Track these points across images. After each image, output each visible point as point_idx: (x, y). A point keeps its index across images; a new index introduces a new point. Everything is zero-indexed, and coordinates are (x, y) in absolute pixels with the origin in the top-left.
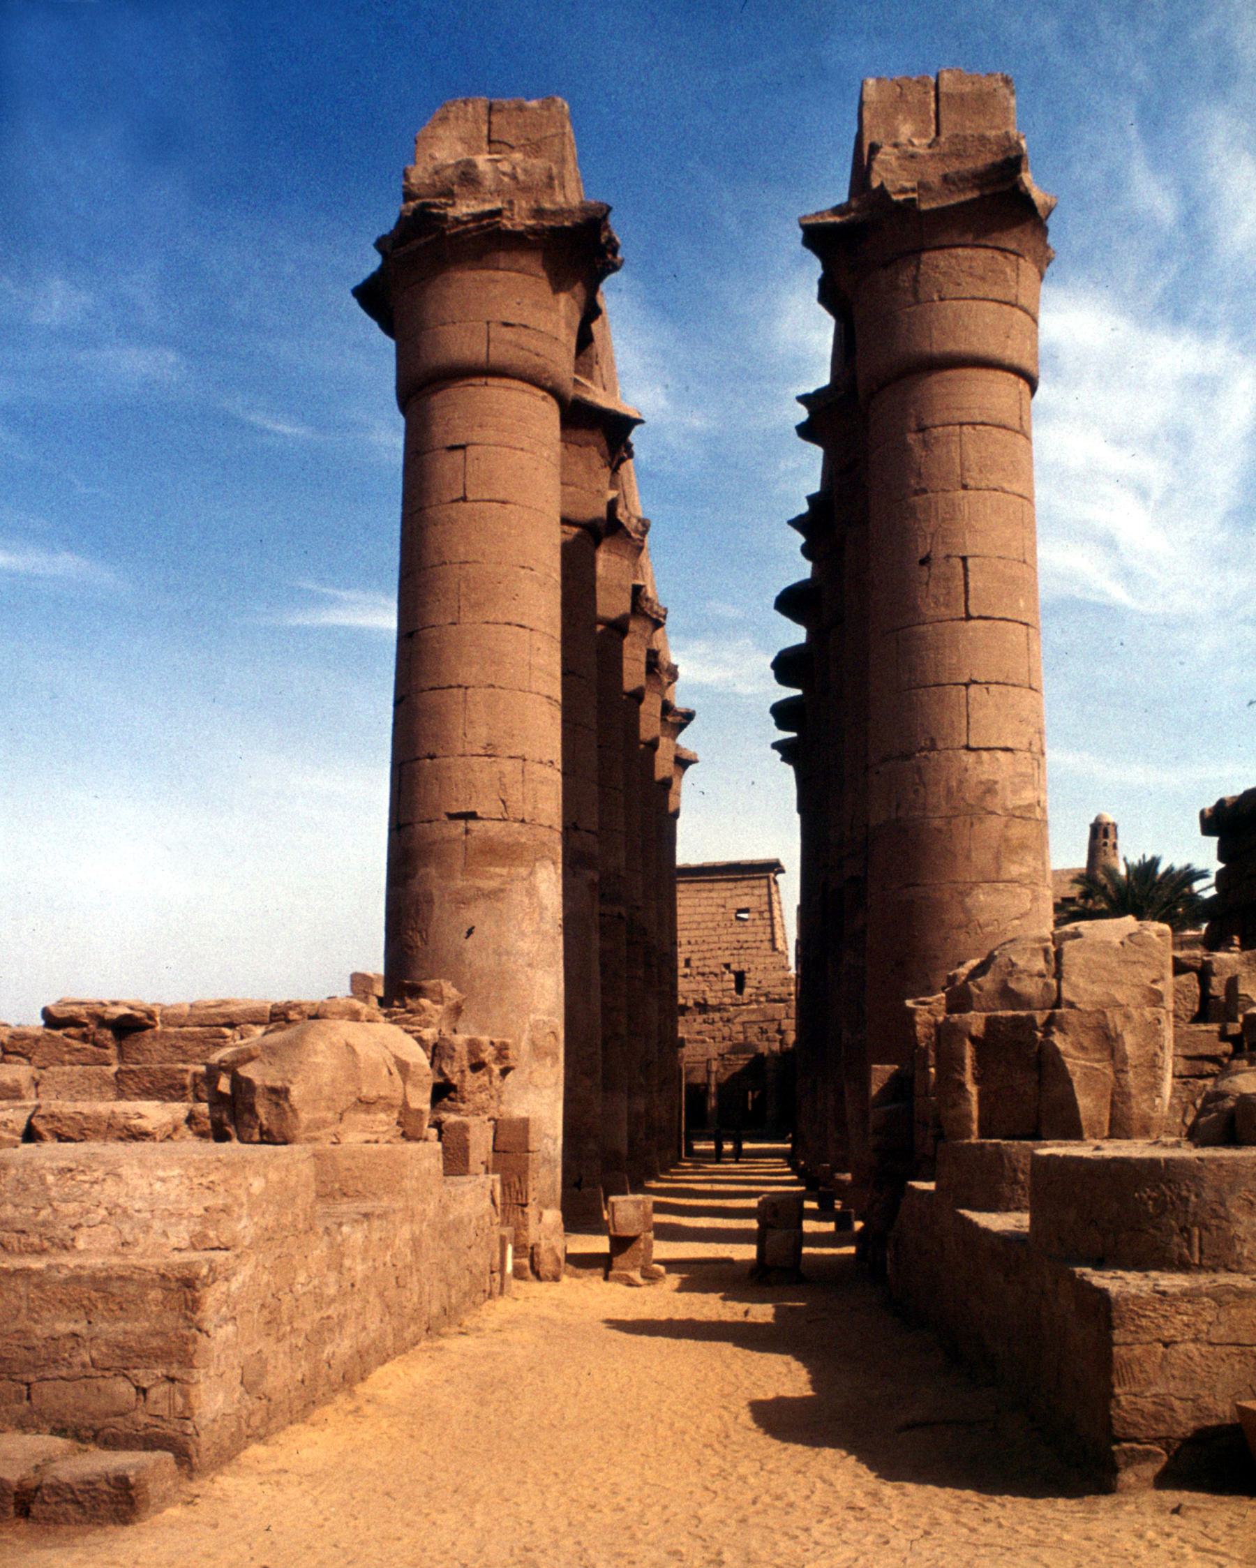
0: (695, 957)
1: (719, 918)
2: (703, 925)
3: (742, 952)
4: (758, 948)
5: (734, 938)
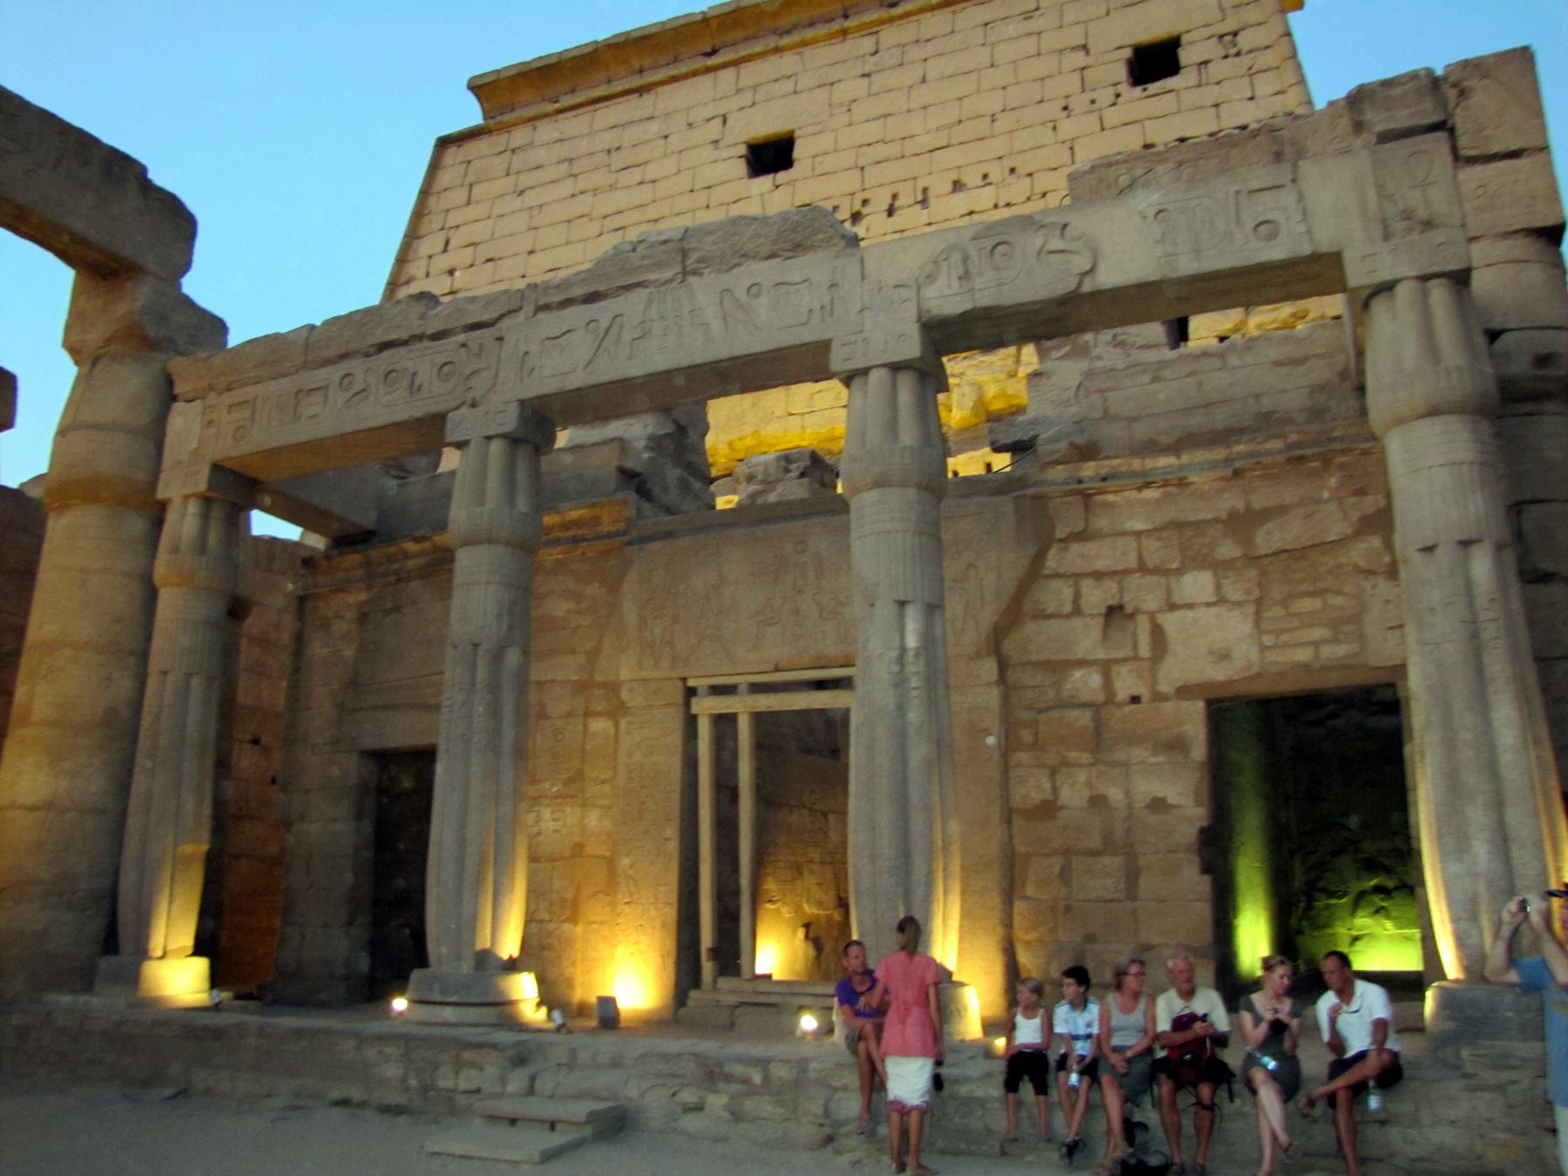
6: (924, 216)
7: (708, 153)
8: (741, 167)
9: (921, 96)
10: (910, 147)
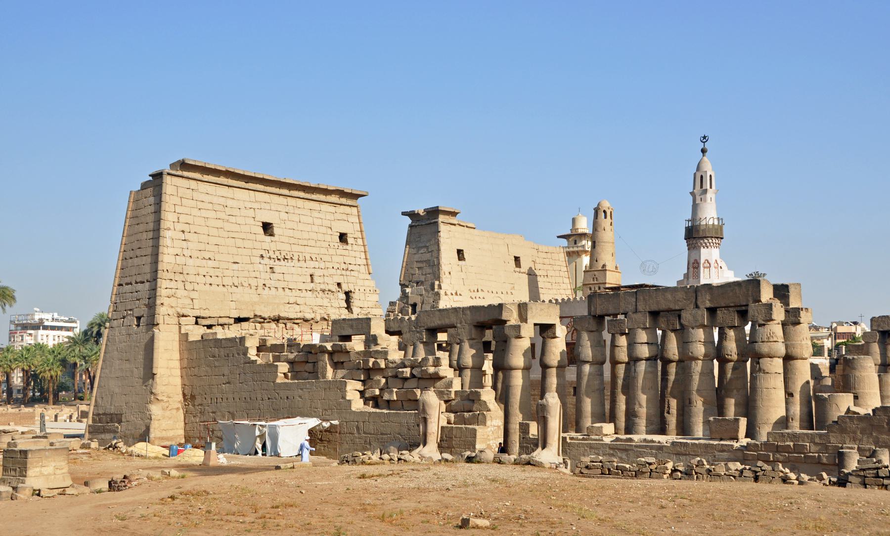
0: (317, 273)
1: (328, 238)
2: (318, 244)
3: (348, 273)
4: (359, 272)
5: (341, 259)
6: (305, 265)
7: (252, 221)
8: (261, 231)
9: (301, 227)
10: (301, 242)
